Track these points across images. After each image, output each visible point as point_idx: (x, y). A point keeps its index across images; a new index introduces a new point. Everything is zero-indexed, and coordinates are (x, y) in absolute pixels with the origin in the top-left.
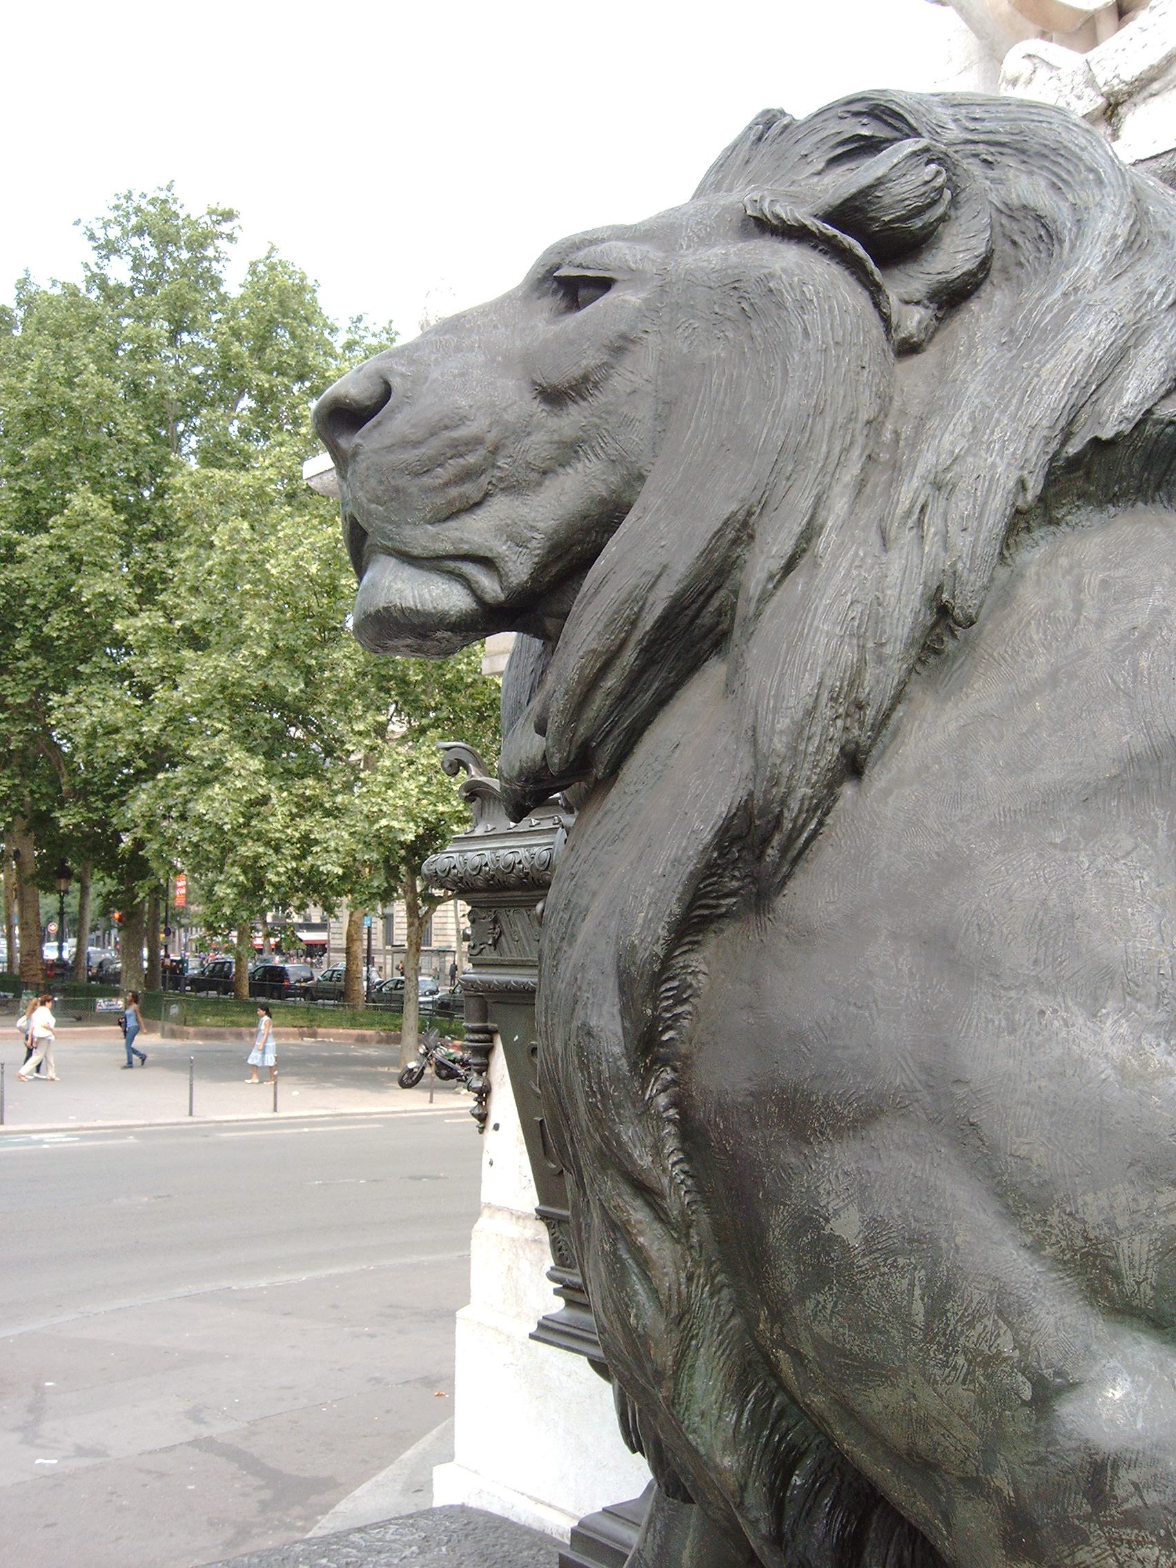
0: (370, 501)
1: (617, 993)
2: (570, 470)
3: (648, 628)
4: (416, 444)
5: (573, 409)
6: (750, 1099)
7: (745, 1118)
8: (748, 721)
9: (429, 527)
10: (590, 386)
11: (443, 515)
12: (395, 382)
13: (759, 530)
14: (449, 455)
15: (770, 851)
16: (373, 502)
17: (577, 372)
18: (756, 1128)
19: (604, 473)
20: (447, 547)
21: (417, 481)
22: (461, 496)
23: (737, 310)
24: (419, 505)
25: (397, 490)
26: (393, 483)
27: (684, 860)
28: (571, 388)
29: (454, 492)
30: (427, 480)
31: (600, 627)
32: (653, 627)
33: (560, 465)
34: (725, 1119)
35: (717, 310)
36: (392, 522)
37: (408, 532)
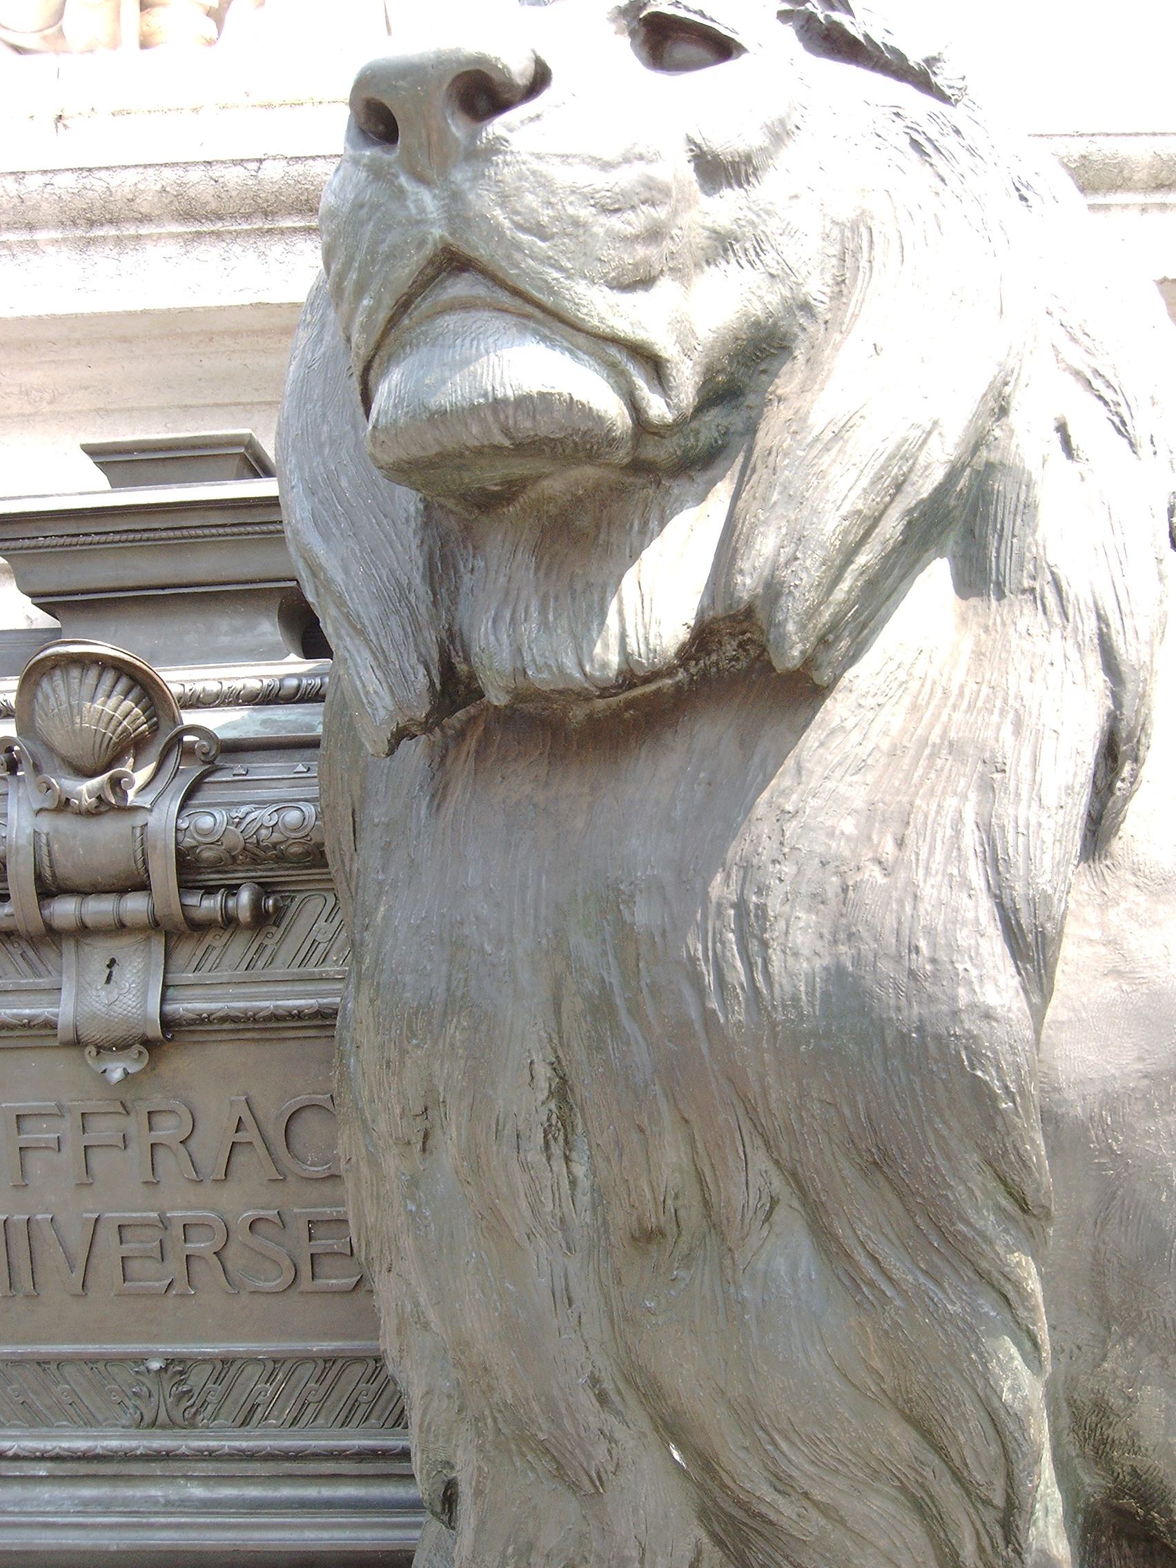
0: (519, 227)
1: (1009, 961)
3: (925, 495)
4: (606, 166)
6: (1146, 1081)
7: (1139, 1106)
8: (1091, 625)
11: (626, 280)
13: (1014, 404)
14: (642, 197)
15: (1119, 784)
18: (1155, 1115)
20: (624, 328)
21: (603, 219)
22: (646, 261)
23: (908, 140)
24: (604, 254)
25: (576, 223)
26: (571, 210)
27: (1077, 789)
28: (733, 163)
29: (641, 251)
31: (865, 482)
32: (930, 495)
33: (708, 263)
34: (1113, 1112)
36: (561, 269)
37: (580, 288)
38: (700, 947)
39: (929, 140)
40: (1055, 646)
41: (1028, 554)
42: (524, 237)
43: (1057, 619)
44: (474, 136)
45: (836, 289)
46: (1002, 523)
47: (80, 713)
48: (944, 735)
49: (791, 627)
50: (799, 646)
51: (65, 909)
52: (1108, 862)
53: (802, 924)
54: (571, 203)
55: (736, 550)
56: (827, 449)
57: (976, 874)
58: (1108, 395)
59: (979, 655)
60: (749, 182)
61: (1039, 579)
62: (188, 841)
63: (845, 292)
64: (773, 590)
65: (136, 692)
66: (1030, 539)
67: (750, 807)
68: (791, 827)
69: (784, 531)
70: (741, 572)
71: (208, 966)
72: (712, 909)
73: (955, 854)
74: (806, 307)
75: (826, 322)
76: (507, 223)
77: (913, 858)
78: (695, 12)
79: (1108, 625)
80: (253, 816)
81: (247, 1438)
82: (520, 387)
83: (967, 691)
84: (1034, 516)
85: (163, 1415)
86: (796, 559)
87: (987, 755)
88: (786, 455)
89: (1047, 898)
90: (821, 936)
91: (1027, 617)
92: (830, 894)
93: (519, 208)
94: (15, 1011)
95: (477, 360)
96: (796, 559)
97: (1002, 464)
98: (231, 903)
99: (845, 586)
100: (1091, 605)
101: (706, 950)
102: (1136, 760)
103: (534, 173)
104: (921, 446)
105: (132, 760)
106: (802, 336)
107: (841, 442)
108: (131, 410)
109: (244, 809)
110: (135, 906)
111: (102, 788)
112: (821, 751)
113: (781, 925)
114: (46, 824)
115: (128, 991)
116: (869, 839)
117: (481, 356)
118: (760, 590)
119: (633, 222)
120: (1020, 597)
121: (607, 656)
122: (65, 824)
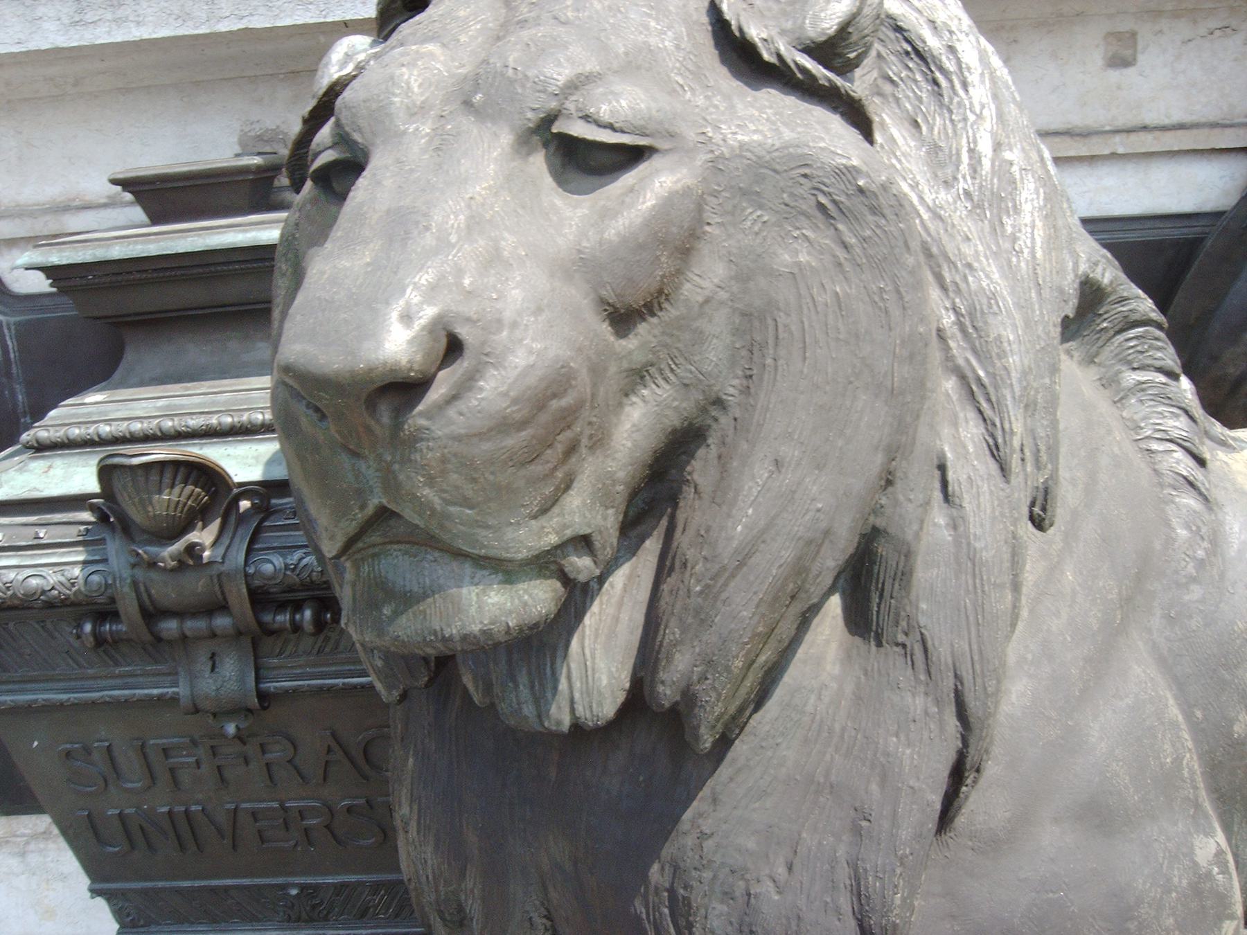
0: (447, 502)
2: (634, 399)
4: (523, 424)
5: (642, 328)
8: (949, 682)
9: (533, 522)
10: (662, 299)
12: (463, 332)
13: (899, 474)
16: (455, 504)
17: (655, 286)
19: (675, 399)
21: (523, 472)
23: (813, 202)
28: (645, 305)
30: (537, 469)
33: (627, 395)
35: (787, 200)
36: (488, 527)
38: (644, 910)
39: (834, 202)
40: (918, 703)
41: (903, 613)
42: (452, 509)
43: (922, 677)
44: (397, 426)
45: (745, 382)
46: (883, 584)
47: (151, 503)
48: (827, 775)
49: (703, 730)
50: (711, 740)
51: (170, 627)
52: (952, 834)
53: (716, 912)
54: (492, 473)
55: (657, 660)
56: (733, 576)
57: (845, 902)
58: (988, 412)
59: (858, 698)
60: (661, 309)
61: (911, 636)
62: (257, 583)
63: (752, 391)
64: (689, 697)
65: (194, 474)
66: (906, 601)
67: (676, 819)
68: (709, 844)
69: (697, 650)
70: (663, 682)
71: (287, 653)
72: (652, 889)
73: (830, 884)
74: (719, 402)
75: (735, 419)
76: (437, 502)
77: (798, 885)
78: (605, 127)
79: (962, 684)
80: (305, 561)
81: (366, 928)
82: (463, 627)
83: (846, 735)
84: (909, 582)
85: (304, 915)
86: (706, 679)
87: (857, 805)
88: (698, 581)
89: (895, 926)
90: (731, 923)
91: (901, 673)
92: (738, 894)
93: (445, 487)
94: (146, 691)
95: (424, 599)
96: (706, 679)
97: (885, 531)
98: (298, 617)
99: (748, 683)
100: (951, 666)
101: (648, 914)
102: (978, 771)
103: (455, 455)
104: (814, 559)
105: (200, 524)
106: (715, 426)
107: (745, 569)
108: (149, 87)
109: (298, 554)
110: (222, 622)
111: (180, 553)
112: (733, 785)
113: (703, 911)
114: (140, 574)
115: (228, 677)
116: (767, 856)
117: (428, 597)
118: (678, 698)
119: (553, 455)
120: (896, 649)
121: (560, 716)
122: (154, 575)
